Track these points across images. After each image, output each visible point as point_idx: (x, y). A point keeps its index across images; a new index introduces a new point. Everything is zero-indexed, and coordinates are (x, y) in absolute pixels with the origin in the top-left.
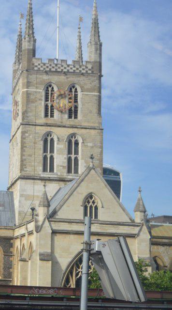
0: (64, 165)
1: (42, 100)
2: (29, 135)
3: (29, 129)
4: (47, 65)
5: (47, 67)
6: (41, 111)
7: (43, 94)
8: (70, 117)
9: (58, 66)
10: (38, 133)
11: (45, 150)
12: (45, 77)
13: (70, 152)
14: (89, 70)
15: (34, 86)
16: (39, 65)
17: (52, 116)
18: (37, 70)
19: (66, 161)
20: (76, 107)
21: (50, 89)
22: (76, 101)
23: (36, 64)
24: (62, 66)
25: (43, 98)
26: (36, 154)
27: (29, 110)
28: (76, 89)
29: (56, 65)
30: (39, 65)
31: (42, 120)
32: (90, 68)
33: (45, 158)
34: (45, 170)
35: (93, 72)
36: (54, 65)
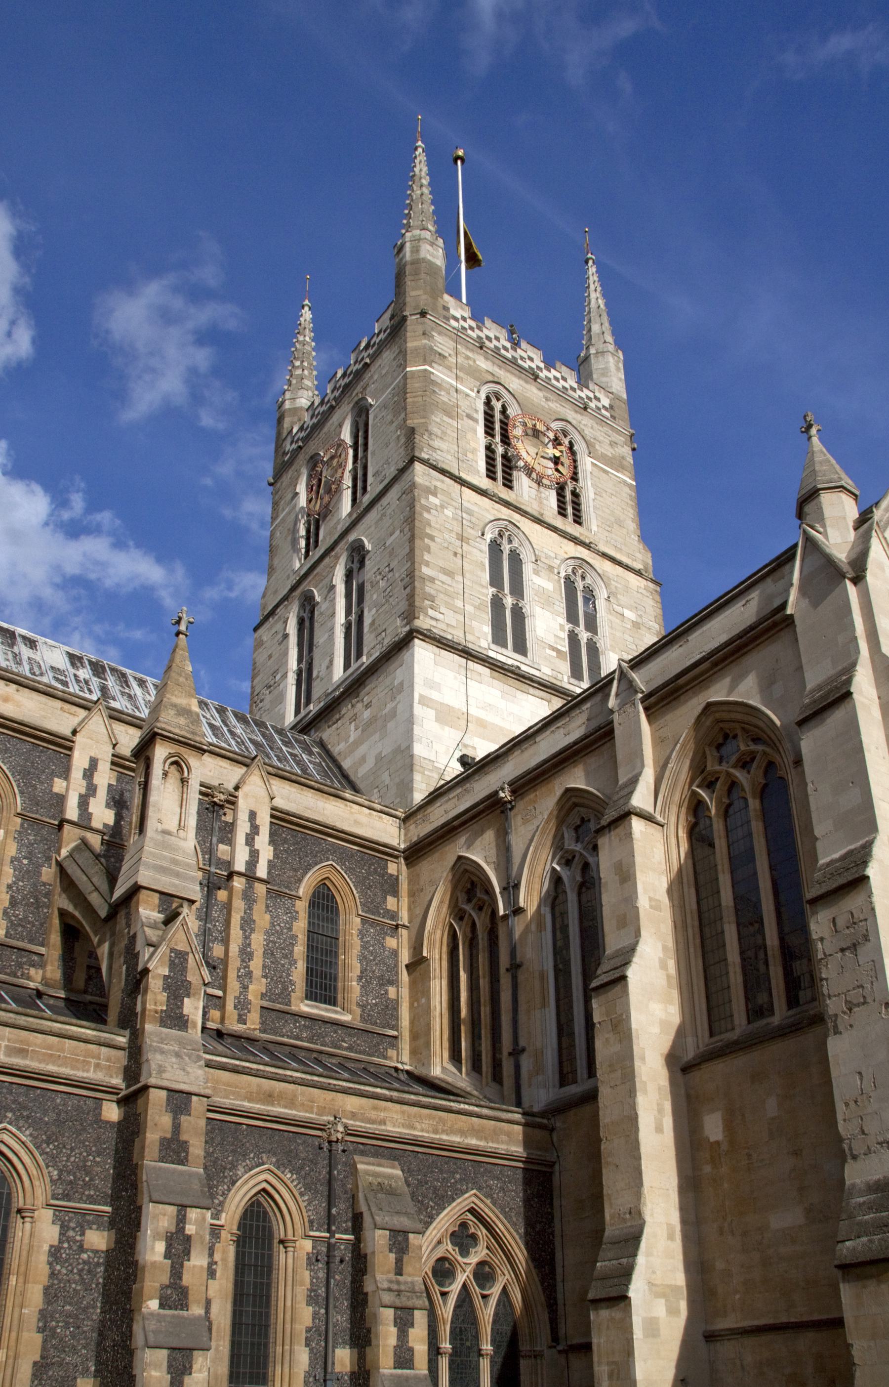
0: (559, 647)
1: (476, 421)
2: (442, 507)
3: (438, 484)
6: (474, 451)
7: (481, 407)
10: (470, 513)
11: (496, 580)
12: (483, 364)
13: (572, 617)
15: (449, 368)
16: (464, 319)
17: (508, 484)
19: (565, 635)
21: (497, 406)
23: (453, 312)
25: (481, 417)
26: (467, 575)
27: (439, 433)
30: (464, 319)
31: (484, 483)
33: (497, 604)
34: (499, 638)
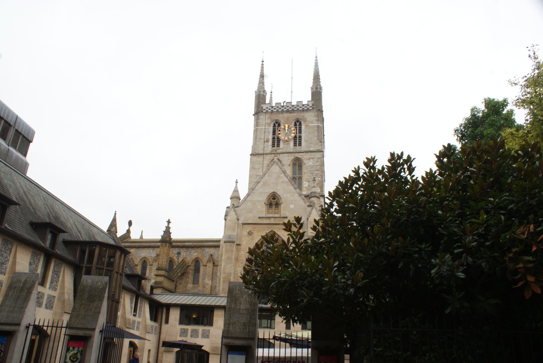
4: (274, 108)
5: (275, 109)
8: (295, 145)
9: (285, 107)
14: (310, 107)
16: (267, 108)
17: (278, 146)
18: (265, 112)
20: (300, 137)
22: (300, 132)
23: (264, 108)
24: (288, 107)
28: (300, 123)
29: (283, 107)
32: (311, 105)
35: (313, 108)
36: (280, 107)
